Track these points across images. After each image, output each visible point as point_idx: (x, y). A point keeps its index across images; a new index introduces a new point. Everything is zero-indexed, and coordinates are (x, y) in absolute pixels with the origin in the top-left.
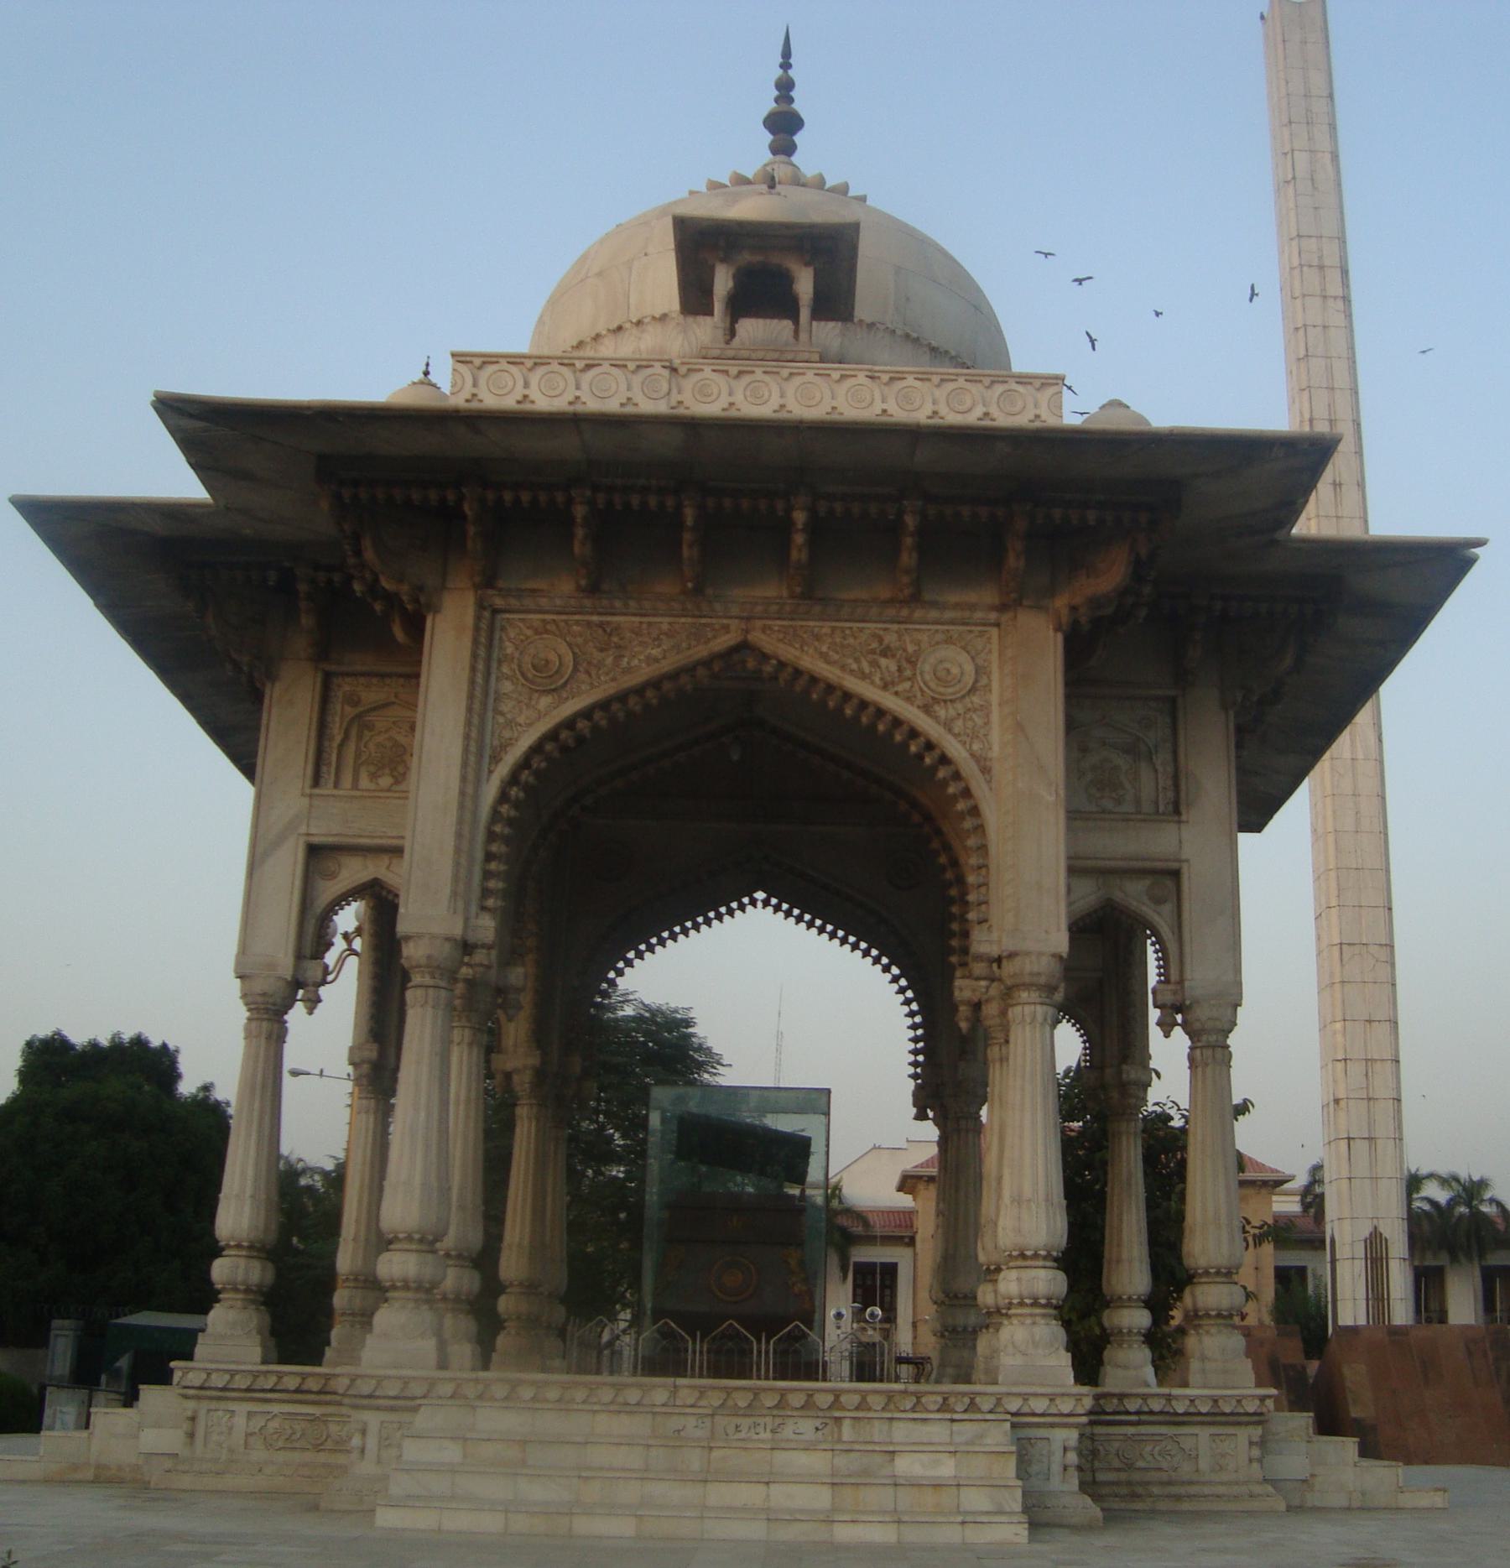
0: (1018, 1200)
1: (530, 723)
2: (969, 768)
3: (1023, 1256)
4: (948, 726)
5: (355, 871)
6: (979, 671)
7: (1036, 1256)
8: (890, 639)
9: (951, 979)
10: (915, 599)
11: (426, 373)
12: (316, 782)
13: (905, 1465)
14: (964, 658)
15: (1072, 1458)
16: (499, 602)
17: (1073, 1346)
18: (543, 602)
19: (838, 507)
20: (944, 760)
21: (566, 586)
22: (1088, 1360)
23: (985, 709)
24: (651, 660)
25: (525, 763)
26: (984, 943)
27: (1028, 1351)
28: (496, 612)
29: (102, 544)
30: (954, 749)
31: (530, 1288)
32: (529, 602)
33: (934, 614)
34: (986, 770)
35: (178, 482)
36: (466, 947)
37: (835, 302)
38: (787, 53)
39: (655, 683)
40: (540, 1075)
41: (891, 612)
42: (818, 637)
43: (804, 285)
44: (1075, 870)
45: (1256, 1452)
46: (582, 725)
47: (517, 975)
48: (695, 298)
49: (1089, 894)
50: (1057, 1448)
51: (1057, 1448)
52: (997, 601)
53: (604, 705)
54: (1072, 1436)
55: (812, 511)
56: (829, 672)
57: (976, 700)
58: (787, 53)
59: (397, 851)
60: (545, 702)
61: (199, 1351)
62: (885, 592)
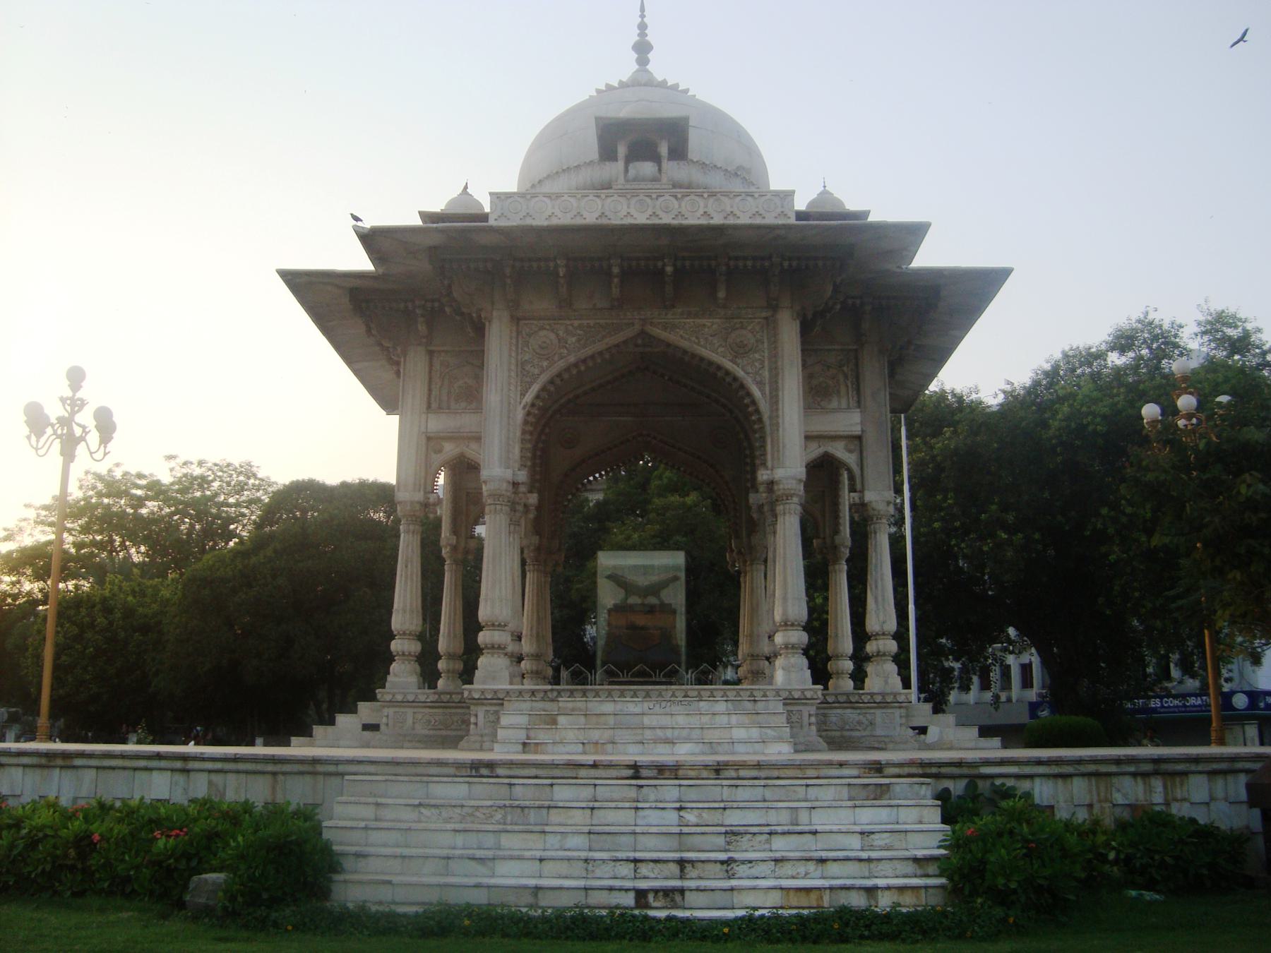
3: (786, 625)
5: (450, 450)
7: (793, 625)
9: (747, 494)
12: (429, 407)
15: (813, 719)
17: (812, 666)
19: (687, 263)
22: (821, 674)
26: (763, 475)
27: (790, 673)
28: (519, 319)
29: (312, 289)
31: (537, 657)
35: (360, 262)
36: (515, 485)
37: (679, 153)
40: (538, 549)
43: (664, 150)
44: (808, 438)
45: (904, 720)
47: (533, 499)
48: (608, 154)
49: (816, 451)
50: (806, 715)
51: (806, 715)
54: (813, 710)
55: (674, 265)
56: (685, 344)
59: (478, 439)
61: (387, 685)
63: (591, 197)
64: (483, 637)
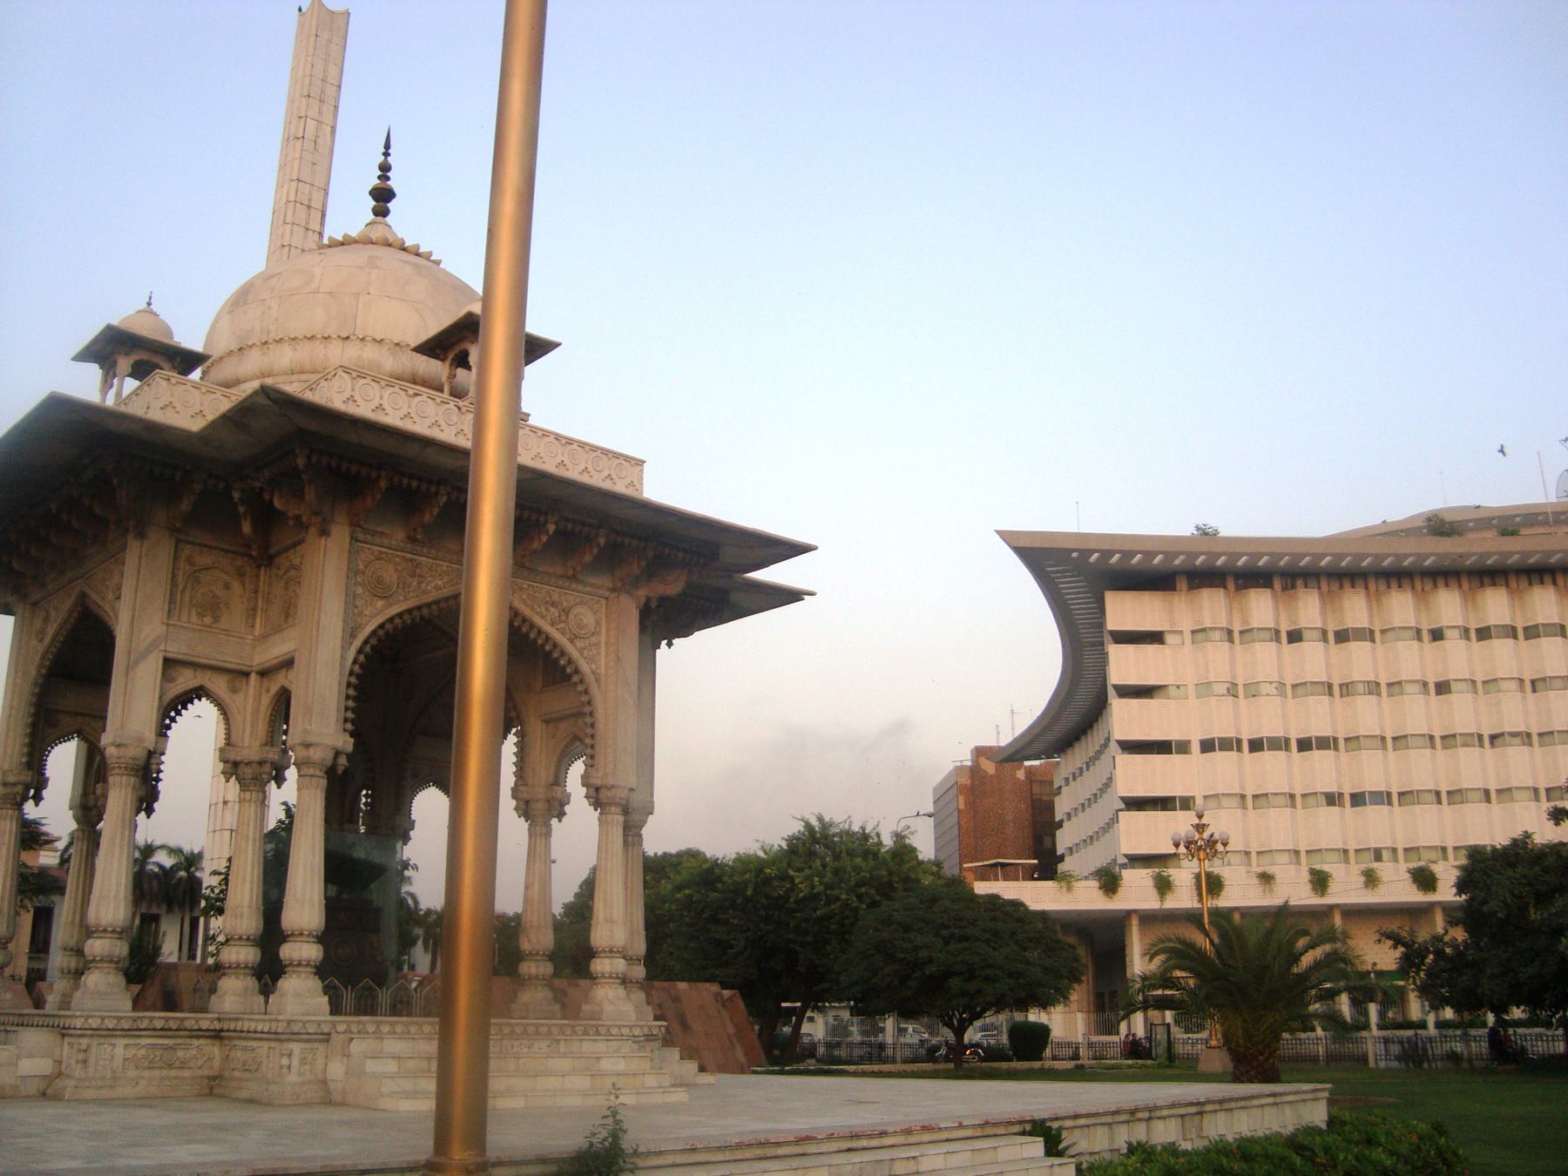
0: (610, 920)
1: (376, 615)
2: (590, 678)
3: (611, 951)
4: (581, 651)
6: (598, 623)
8: (555, 597)
10: (574, 578)
11: (149, 304)
13: (606, 1065)
14: (589, 614)
16: (361, 536)
18: (386, 541)
20: (577, 671)
21: (400, 535)
23: (597, 645)
24: (438, 588)
25: (366, 642)
30: (585, 667)
32: (377, 540)
33: (580, 587)
34: (597, 680)
38: (387, 146)
39: (437, 602)
41: (560, 582)
42: (521, 589)
46: (398, 621)
52: (610, 585)
53: (410, 611)
57: (593, 640)
58: (387, 146)
60: (380, 603)
62: (560, 570)
63: (424, 397)
64: (288, 951)
